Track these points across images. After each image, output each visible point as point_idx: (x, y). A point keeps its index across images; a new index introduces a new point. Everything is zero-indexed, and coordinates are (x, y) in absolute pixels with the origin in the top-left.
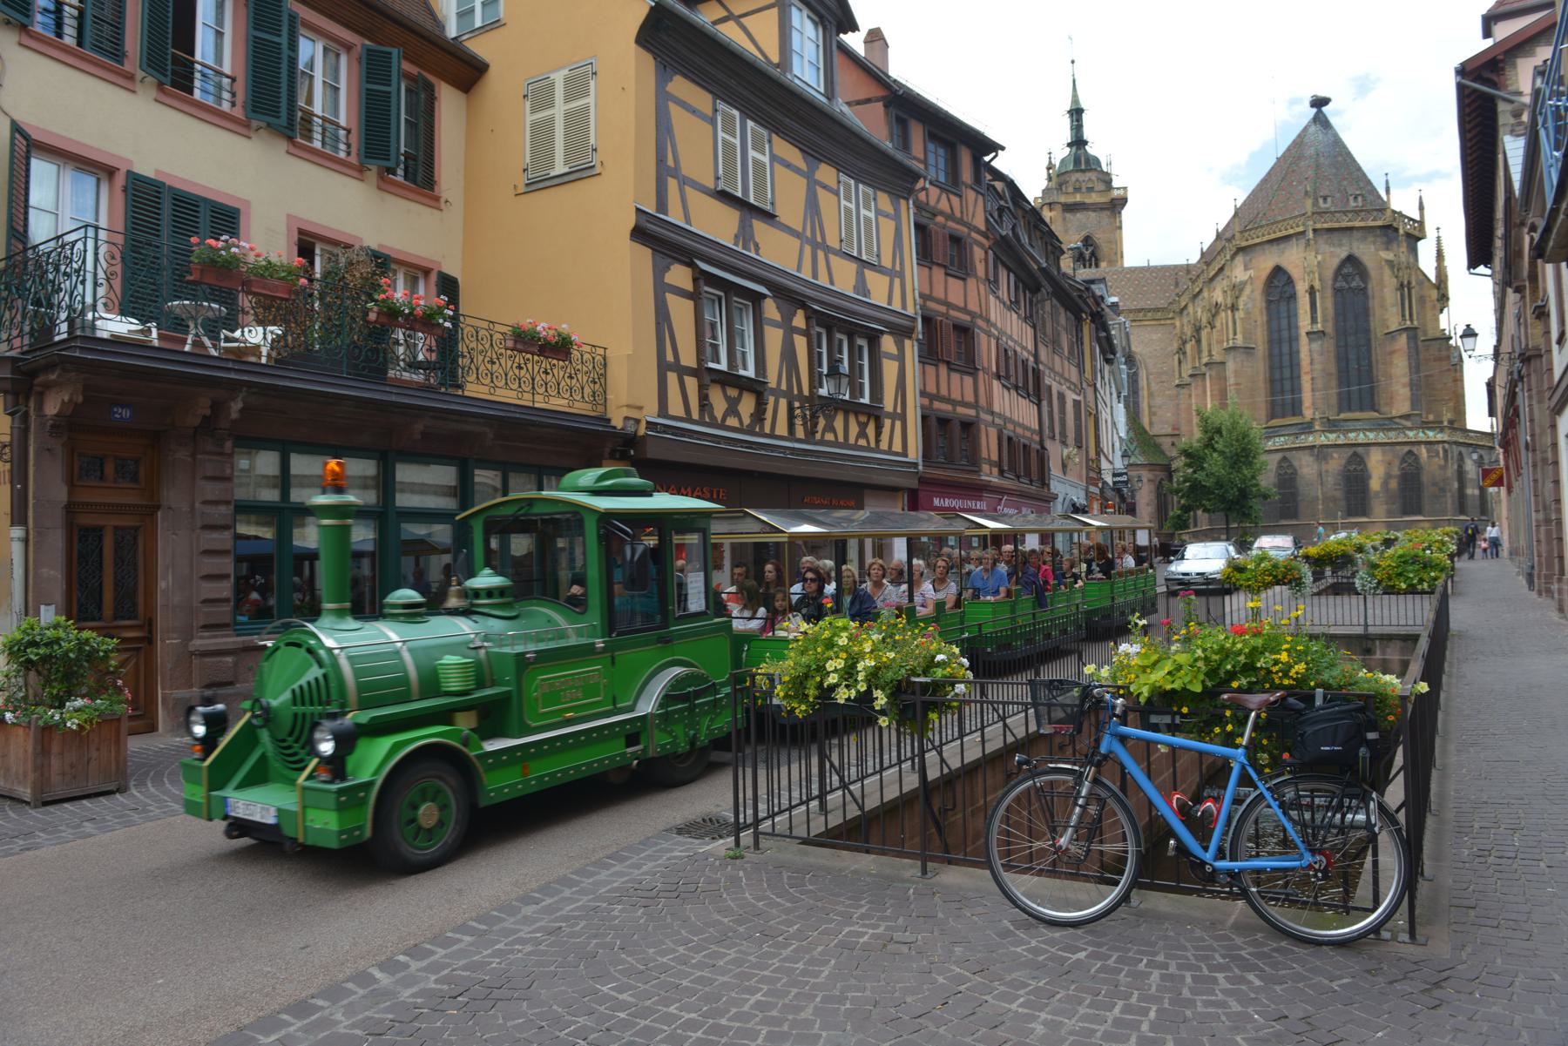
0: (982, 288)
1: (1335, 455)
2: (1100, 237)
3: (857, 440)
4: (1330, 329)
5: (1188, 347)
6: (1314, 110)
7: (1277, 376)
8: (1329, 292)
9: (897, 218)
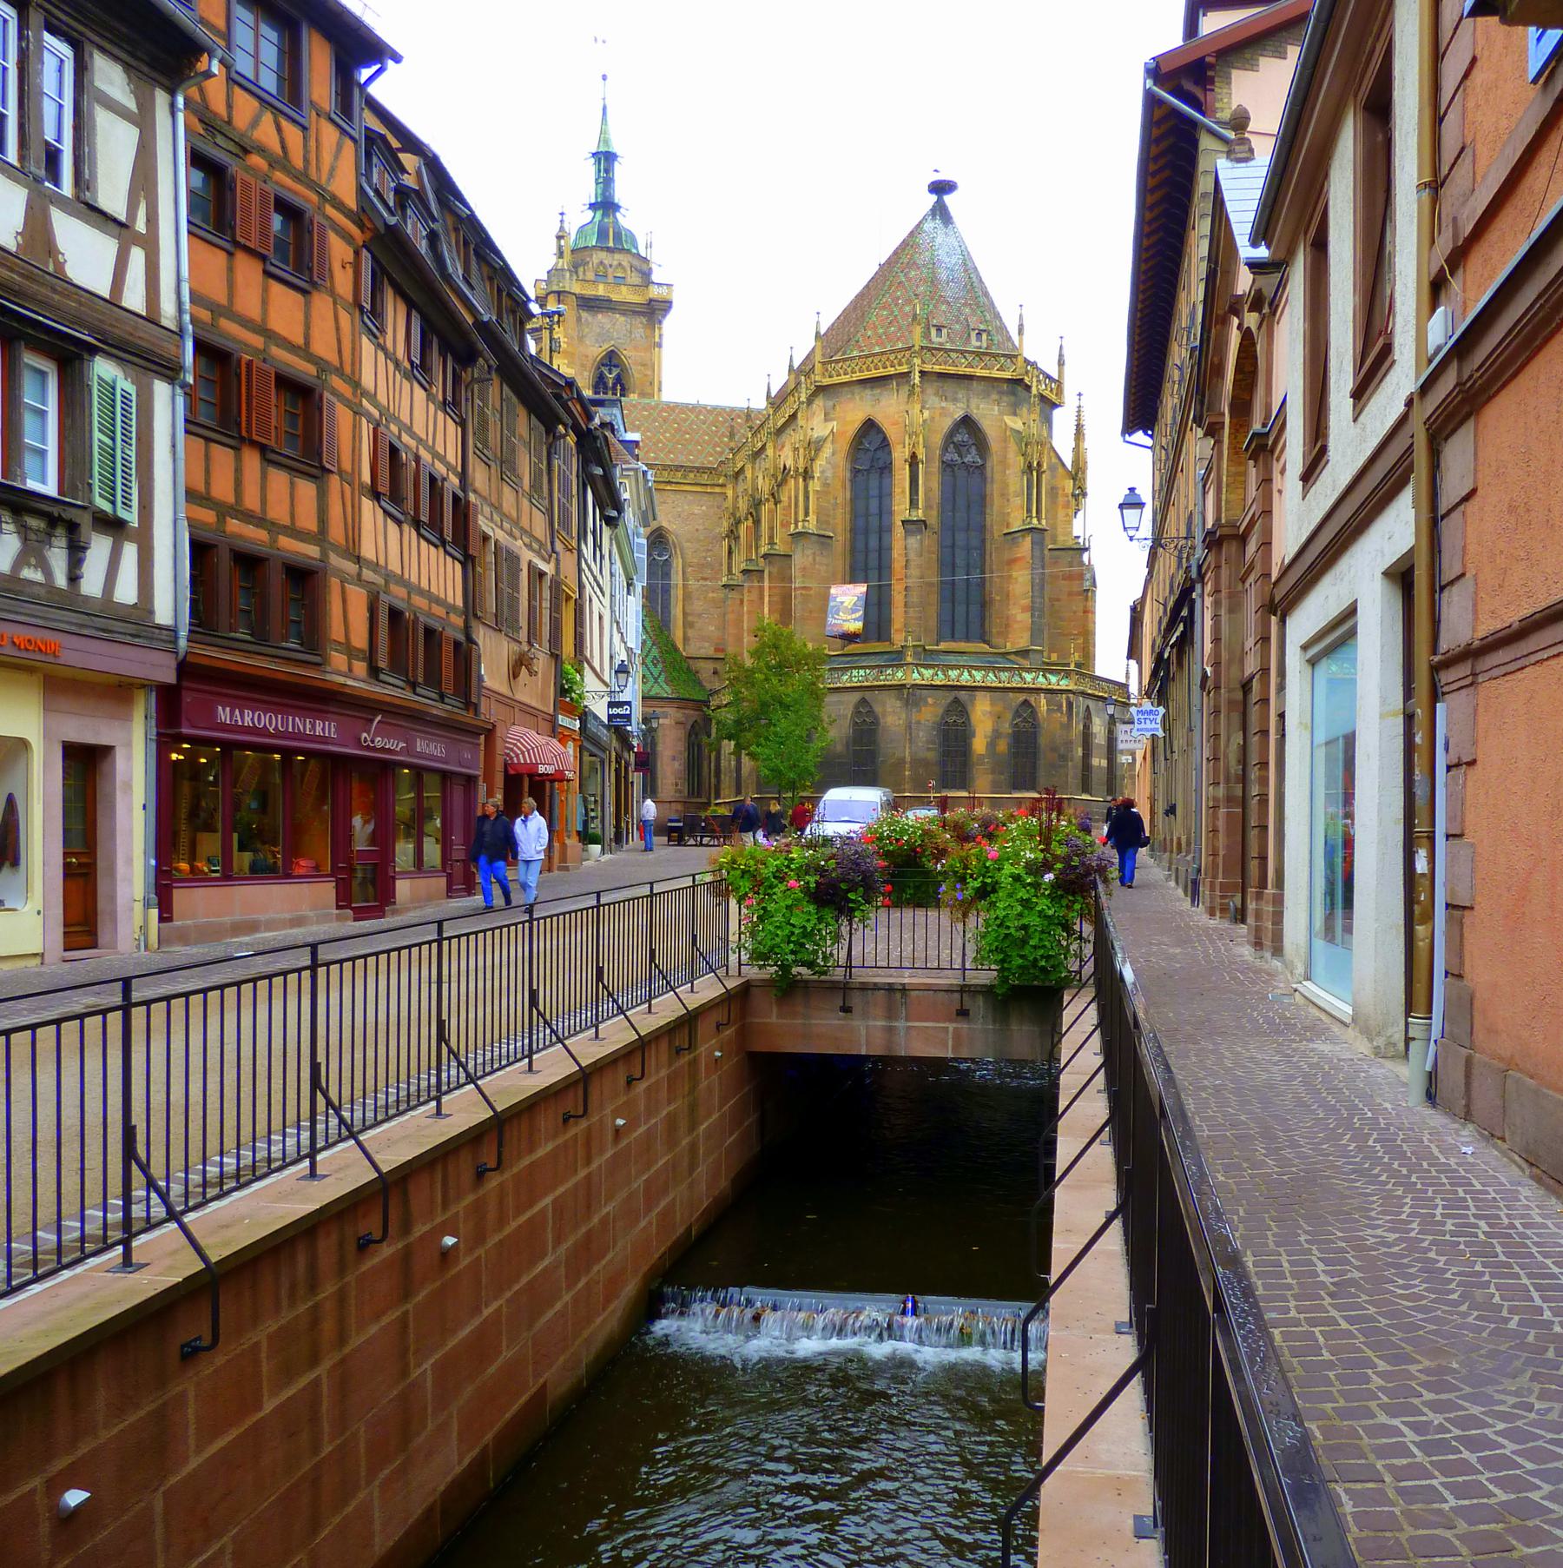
2: (629, 355)
4: (933, 520)
6: (934, 198)
8: (936, 464)
9: (143, 120)
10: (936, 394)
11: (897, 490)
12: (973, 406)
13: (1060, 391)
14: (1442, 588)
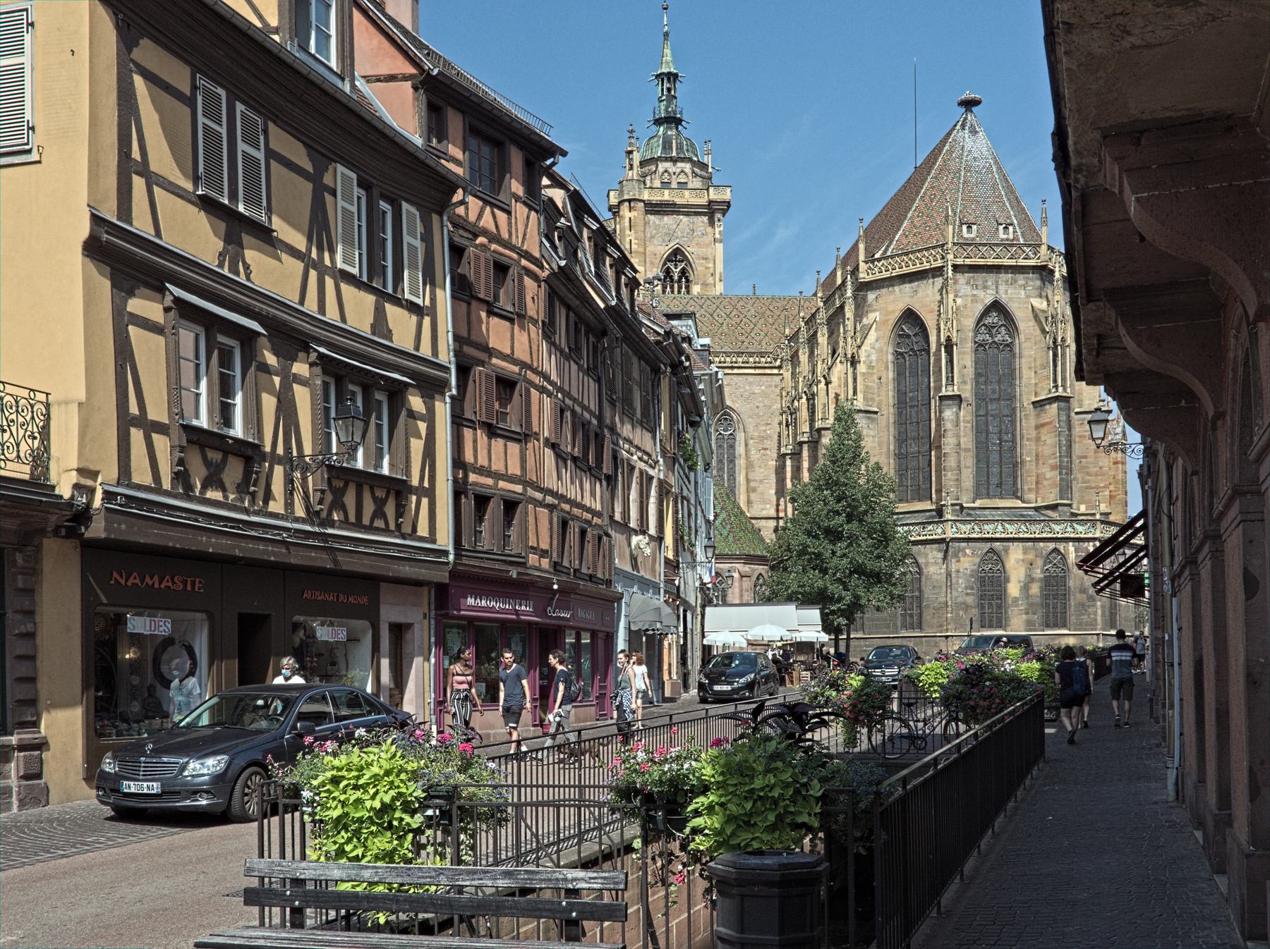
4: (967, 393)
8: (969, 346)
10: (968, 283)
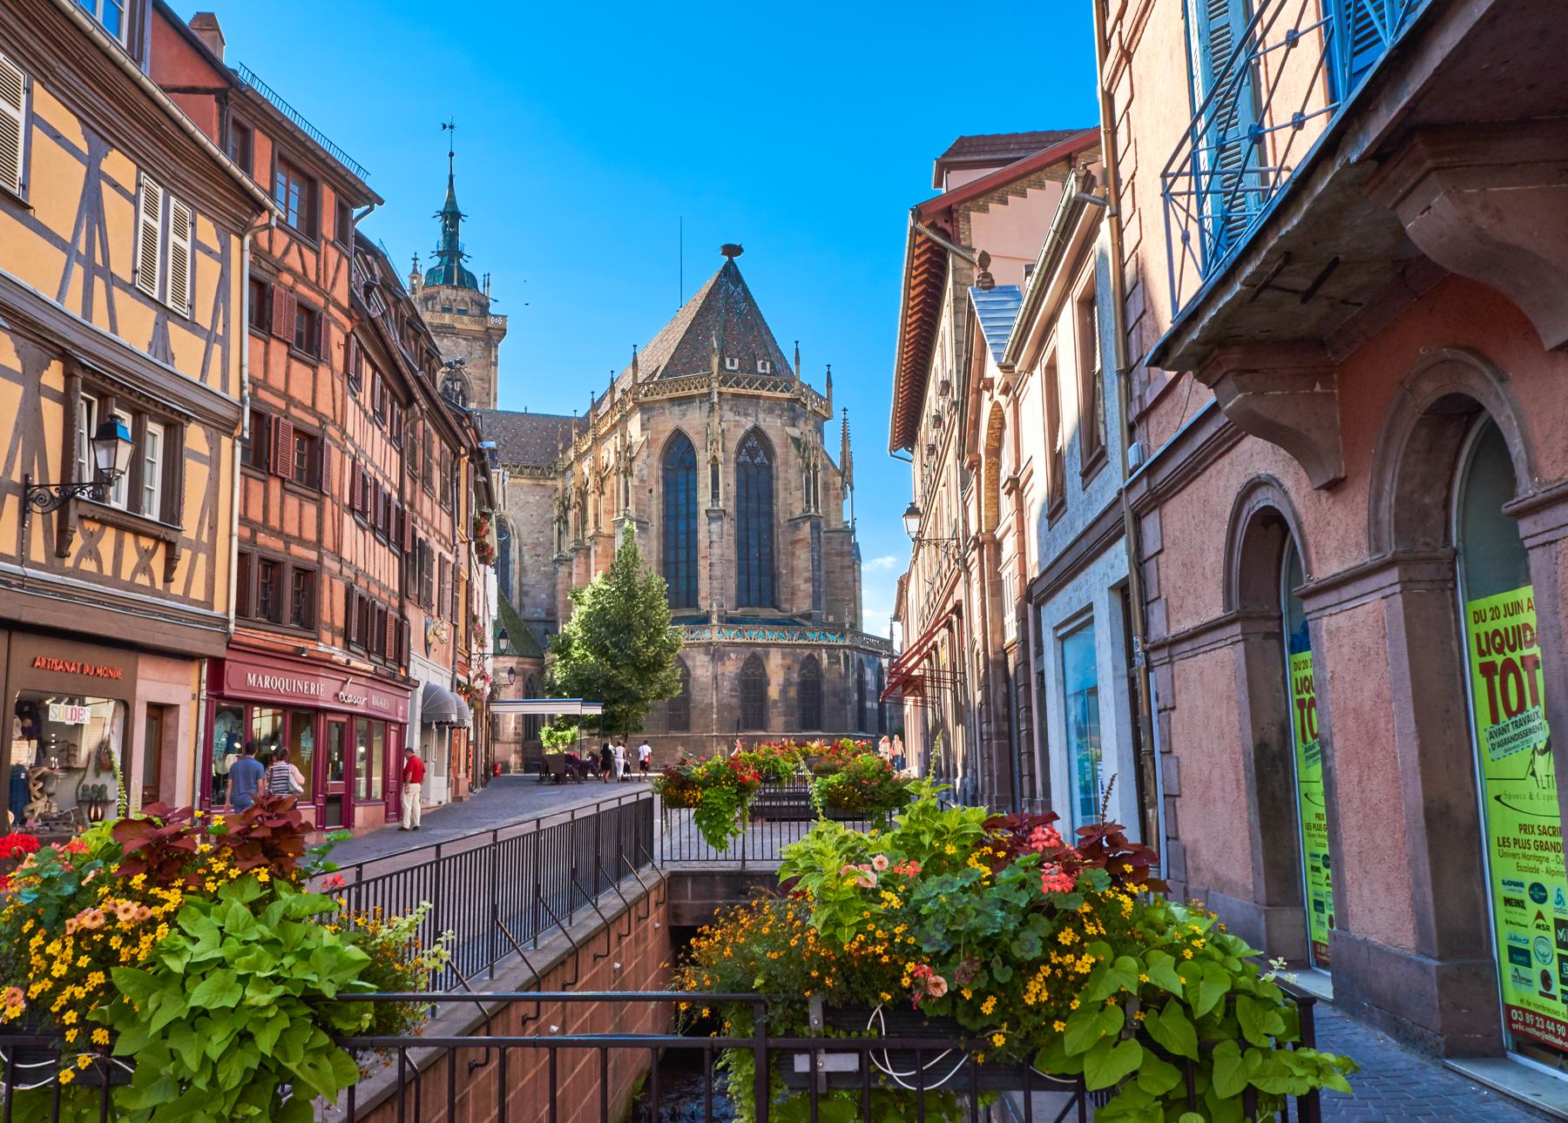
0: (338, 384)
1: (732, 655)
3: (134, 575)
4: (731, 509)
5: (571, 515)
6: (726, 258)
7: (672, 559)
8: (732, 465)
9: (224, 258)
10: (731, 410)
11: (701, 485)
12: (761, 420)
13: (828, 408)
14: (1148, 604)
